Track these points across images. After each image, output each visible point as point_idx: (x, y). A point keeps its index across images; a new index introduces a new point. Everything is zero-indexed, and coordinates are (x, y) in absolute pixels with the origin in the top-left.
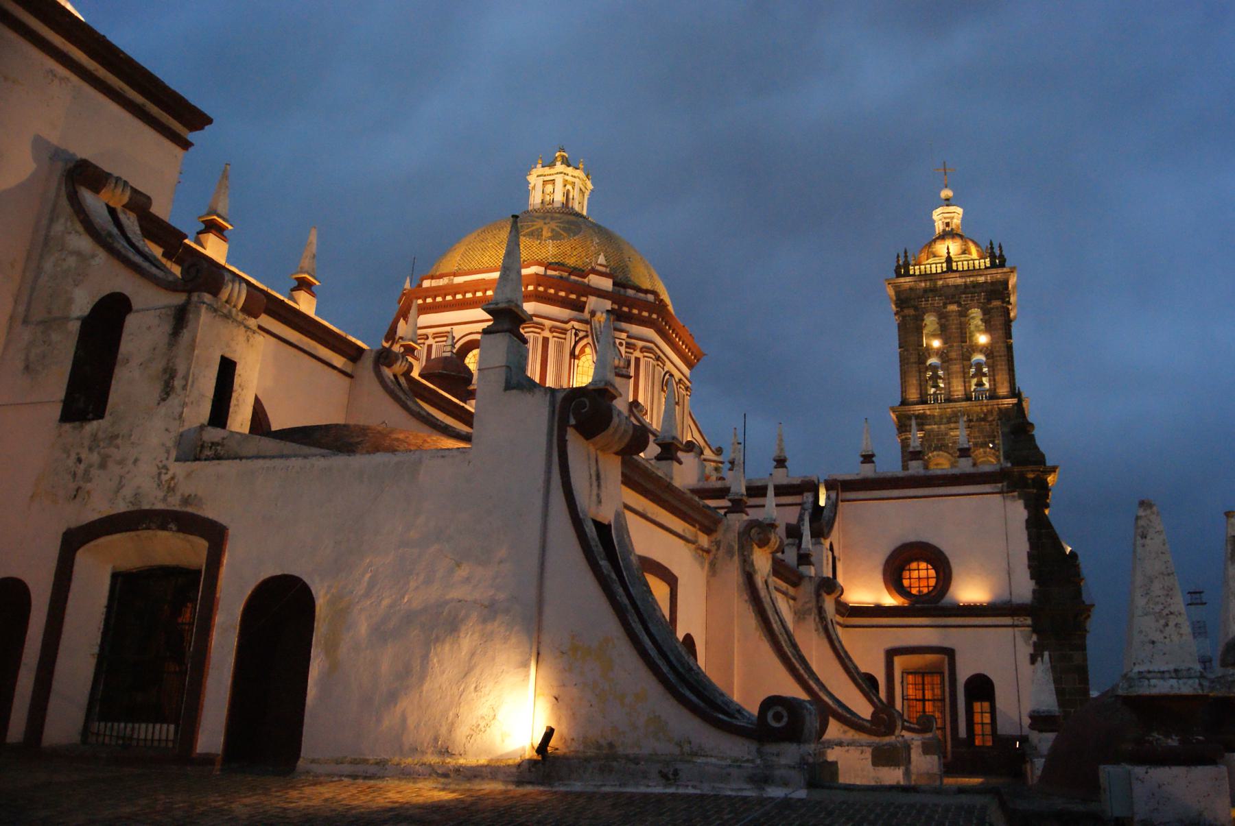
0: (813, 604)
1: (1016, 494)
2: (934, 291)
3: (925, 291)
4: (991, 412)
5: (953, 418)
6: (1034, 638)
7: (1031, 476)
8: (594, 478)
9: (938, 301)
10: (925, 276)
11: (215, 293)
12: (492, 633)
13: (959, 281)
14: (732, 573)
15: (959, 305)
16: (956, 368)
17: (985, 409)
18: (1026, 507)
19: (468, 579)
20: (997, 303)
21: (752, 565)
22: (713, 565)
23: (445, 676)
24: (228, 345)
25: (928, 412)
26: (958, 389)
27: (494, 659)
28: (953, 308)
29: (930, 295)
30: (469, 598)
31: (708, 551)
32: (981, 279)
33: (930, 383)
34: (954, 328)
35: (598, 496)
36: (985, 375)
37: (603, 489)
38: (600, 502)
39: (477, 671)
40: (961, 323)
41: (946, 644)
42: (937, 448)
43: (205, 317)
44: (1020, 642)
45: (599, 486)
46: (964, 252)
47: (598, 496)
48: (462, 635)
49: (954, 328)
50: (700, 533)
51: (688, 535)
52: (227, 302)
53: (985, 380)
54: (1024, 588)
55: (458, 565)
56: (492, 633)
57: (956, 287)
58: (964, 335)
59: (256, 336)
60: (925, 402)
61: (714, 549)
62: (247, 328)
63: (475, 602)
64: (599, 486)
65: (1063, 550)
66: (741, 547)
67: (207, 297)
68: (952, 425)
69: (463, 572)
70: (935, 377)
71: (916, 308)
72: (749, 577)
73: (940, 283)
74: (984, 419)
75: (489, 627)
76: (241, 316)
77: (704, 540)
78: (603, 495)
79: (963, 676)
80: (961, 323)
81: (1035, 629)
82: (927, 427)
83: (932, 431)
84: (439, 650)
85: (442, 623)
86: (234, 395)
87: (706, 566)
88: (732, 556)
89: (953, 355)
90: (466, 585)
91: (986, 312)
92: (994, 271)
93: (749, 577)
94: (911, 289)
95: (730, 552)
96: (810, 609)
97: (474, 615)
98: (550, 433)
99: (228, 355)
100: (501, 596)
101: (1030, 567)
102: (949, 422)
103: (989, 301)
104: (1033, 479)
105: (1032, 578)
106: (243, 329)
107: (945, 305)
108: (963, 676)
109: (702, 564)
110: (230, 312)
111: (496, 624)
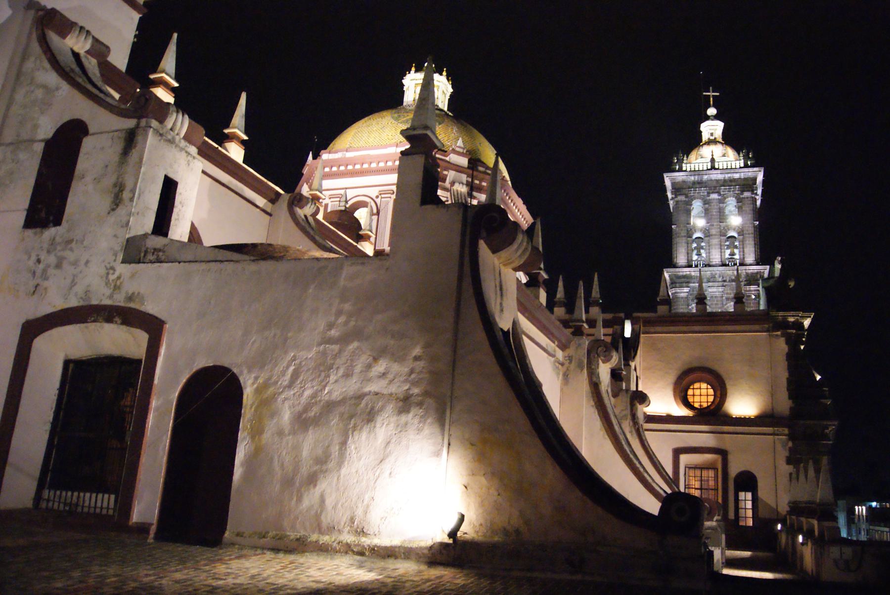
0: (628, 412)
1: (779, 333)
2: (700, 184)
3: (694, 183)
5: (712, 279)
6: (790, 444)
7: (791, 319)
8: (498, 288)
9: (703, 191)
10: (694, 172)
11: (162, 121)
12: (406, 424)
13: (720, 177)
14: (582, 382)
15: (720, 194)
16: (715, 241)
18: (787, 343)
19: (384, 374)
20: (747, 194)
21: (598, 377)
22: (566, 376)
23: (362, 462)
24: (171, 166)
26: (716, 258)
27: (407, 447)
28: (714, 196)
30: (385, 392)
31: (562, 364)
32: (737, 176)
33: (695, 252)
34: (714, 212)
35: (501, 304)
36: (736, 247)
37: (504, 298)
38: (502, 310)
39: (391, 459)
40: (720, 208)
41: (723, 447)
43: (151, 138)
44: (779, 447)
45: (502, 295)
46: (724, 156)
47: (501, 304)
48: (378, 425)
49: (714, 212)
50: (557, 349)
51: (549, 349)
52: (171, 129)
53: (736, 251)
54: (784, 404)
55: (375, 359)
56: (406, 424)
57: (717, 181)
58: (722, 217)
59: (195, 161)
60: (690, 266)
61: (567, 365)
62: (188, 154)
63: (391, 394)
64: (502, 295)
65: (815, 378)
66: (589, 363)
67: (154, 123)
68: (710, 284)
69: (380, 367)
70: (699, 248)
71: (687, 196)
72: (595, 386)
73: (705, 177)
75: (404, 418)
76: (183, 144)
77: (560, 354)
78: (504, 305)
79: (733, 471)
80: (720, 208)
81: (792, 437)
82: (691, 285)
84: (356, 438)
85: (360, 412)
86: (175, 210)
87: (561, 376)
88: (582, 370)
89: (714, 231)
90: (387, 377)
91: (739, 200)
92: (746, 170)
93: (595, 386)
94: (684, 182)
95: (580, 366)
96: (625, 416)
97: (390, 408)
98: (462, 246)
99: (171, 175)
100: (416, 391)
101: (788, 390)
103: (742, 192)
104: (793, 322)
105: (790, 398)
106: (185, 154)
107: (709, 194)
108: (733, 471)
109: (558, 374)
110: (174, 138)
111: (411, 415)
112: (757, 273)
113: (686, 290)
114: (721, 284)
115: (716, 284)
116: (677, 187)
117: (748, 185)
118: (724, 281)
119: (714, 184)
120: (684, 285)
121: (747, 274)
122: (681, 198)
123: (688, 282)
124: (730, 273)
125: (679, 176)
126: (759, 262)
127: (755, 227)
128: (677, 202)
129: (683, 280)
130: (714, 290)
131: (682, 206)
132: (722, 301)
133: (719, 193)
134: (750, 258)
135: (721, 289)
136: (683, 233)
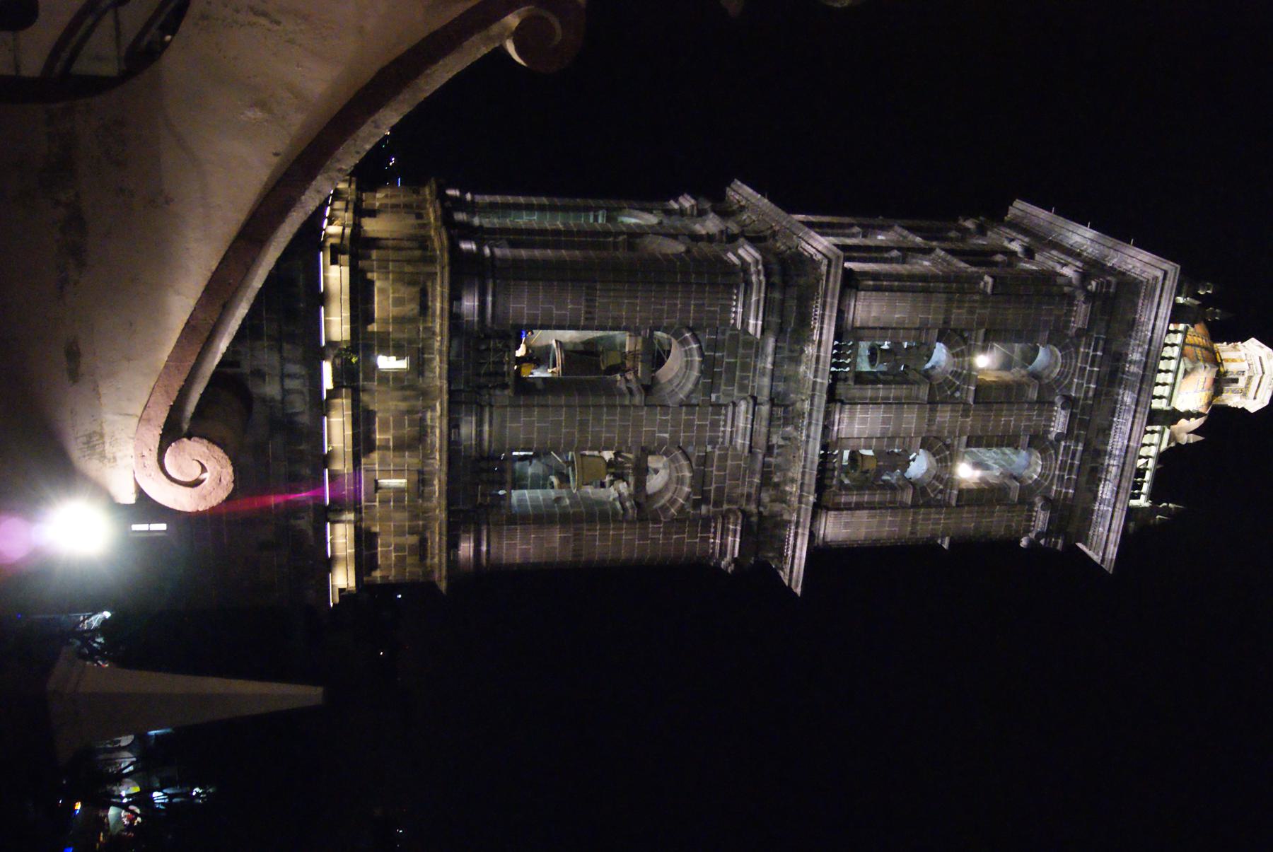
2: (1112, 376)
4: (782, 498)
5: (782, 408)
9: (1083, 387)
17: (793, 489)
25: (810, 350)
29: (1105, 369)
34: (1009, 419)
42: (709, 367)
57: (1105, 431)
60: (838, 336)
68: (765, 409)
71: (1080, 333)
73: (1128, 398)
74: (766, 480)
82: (771, 343)
83: (756, 348)
89: (945, 416)
91: (1027, 493)
102: (776, 400)
103: (1049, 503)
107: (1069, 402)
112: (781, 556)
113: (755, 325)
114: (762, 440)
115: (762, 428)
117: (1072, 516)
118: (769, 449)
119: (1099, 421)
120: (775, 320)
122: (1080, 315)
123: (780, 333)
124: (796, 471)
125: (1155, 317)
126: (820, 554)
128: (1070, 299)
132: (700, 443)
133: (1068, 435)
134: (833, 528)
136: (959, 315)
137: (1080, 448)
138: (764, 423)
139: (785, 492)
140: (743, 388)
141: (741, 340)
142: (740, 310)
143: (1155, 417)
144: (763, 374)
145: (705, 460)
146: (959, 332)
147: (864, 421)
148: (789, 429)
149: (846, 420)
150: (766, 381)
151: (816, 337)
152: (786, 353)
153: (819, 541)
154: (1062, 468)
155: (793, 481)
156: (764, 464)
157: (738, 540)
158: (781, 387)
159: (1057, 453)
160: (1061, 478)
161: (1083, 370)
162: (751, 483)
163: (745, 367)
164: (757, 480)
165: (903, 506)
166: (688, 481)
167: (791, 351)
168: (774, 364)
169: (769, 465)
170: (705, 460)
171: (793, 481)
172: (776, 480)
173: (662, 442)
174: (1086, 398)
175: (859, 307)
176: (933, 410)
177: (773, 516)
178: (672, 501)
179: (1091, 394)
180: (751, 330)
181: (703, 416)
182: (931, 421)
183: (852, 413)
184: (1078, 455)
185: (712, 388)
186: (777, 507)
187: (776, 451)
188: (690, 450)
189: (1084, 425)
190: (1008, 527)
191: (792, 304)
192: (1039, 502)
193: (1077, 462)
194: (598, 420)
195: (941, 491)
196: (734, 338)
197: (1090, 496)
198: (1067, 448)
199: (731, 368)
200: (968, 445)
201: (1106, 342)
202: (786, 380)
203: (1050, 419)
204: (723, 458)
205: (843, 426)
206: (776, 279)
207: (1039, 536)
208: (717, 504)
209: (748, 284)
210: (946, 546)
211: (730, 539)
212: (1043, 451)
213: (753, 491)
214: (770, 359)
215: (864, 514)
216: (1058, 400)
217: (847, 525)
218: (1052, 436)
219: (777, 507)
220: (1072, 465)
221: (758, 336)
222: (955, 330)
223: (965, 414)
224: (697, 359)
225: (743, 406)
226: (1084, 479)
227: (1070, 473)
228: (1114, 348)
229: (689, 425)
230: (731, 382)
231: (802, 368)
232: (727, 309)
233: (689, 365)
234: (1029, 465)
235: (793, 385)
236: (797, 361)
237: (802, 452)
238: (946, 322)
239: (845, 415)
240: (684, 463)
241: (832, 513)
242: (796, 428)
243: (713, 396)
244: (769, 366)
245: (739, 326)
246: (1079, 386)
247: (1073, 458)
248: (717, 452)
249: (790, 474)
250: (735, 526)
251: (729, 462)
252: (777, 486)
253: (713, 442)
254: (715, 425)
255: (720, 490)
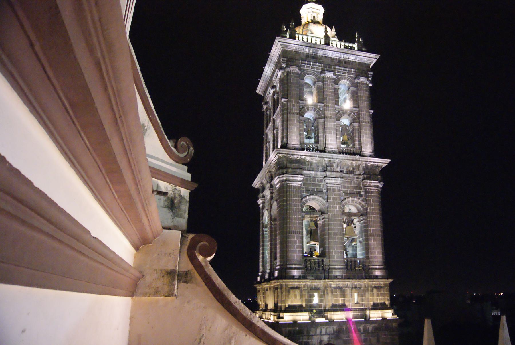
2: (314, 58)
3: (308, 56)
4: (358, 167)
9: (318, 67)
17: (355, 164)
25: (308, 159)
28: (329, 75)
29: (311, 60)
34: (329, 91)
42: (315, 192)
57: (332, 59)
60: (303, 149)
68: (328, 173)
73: (321, 52)
82: (306, 172)
83: (308, 176)
89: (328, 113)
94: (296, 52)
103: (357, 77)
107: (323, 72)
112: (378, 167)
113: (300, 178)
114: (339, 174)
116: (289, 56)
117: (361, 69)
118: (341, 171)
119: (329, 61)
120: (298, 171)
121: (367, 166)
122: (294, 69)
125: (293, 45)
126: (377, 153)
127: (370, 116)
128: (288, 73)
129: (297, 165)
130: (332, 181)
131: (294, 80)
134: (368, 149)
135: (339, 181)
136: (295, 110)
137: (338, 67)
138: (333, 173)
139: (356, 166)
140: (321, 181)
141: (305, 182)
142: (295, 183)
143: (327, 43)
144: (316, 174)
145: (346, 193)
146: (300, 110)
147: (331, 140)
148: (334, 165)
149: (331, 146)
150: (319, 173)
151: (303, 157)
152: (309, 167)
153: (372, 154)
154: (345, 73)
155: (352, 163)
156: (347, 173)
157: (372, 181)
158: (320, 168)
159: (340, 75)
160: (348, 74)
161: (312, 68)
162: (354, 178)
163: (314, 180)
164: (352, 175)
165: (359, 126)
166: (353, 199)
167: (308, 165)
168: (313, 171)
169: (347, 171)
170: (346, 193)
171: (352, 163)
172: (352, 169)
173: (340, 208)
174: (321, 66)
175: (293, 143)
176: (327, 117)
177: (364, 169)
178: (360, 204)
179: (320, 65)
180: (302, 179)
181: (331, 194)
182: (330, 118)
183: (328, 144)
184: (341, 68)
185: (322, 192)
186: (361, 169)
187: (342, 169)
188: (342, 198)
189: (330, 66)
190: (366, 91)
191: (293, 165)
192: (356, 81)
193: (343, 68)
194: (333, 229)
195: (354, 114)
196: (304, 184)
197: (354, 64)
198: (338, 72)
199: (315, 185)
200: (338, 105)
201: (302, 60)
202: (318, 167)
203: (329, 78)
204: (345, 187)
205: (333, 147)
206: (285, 171)
207: (368, 80)
208: (360, 188)
209: (286, 180)
210: (372, 111)
211: (372, 184)
212: (339, 80)
213: (356, 177)
214: (311, 172)
215: (362, 139)
216: (322, 75)
217: (366, 145)
218: (335, 77)
219: (361, 169)
220: (344, 70)
221: (303, 176)
222: (300, 111)
223: (328, 106)
224: (312, 197)
225: (327, 181)
226: (349, 66)
227: (347, 71)
228: (304, 58)
229: (334, 199)
230: (319, 185)
231: (314, 161)
232: (295, 187)
233: (314, 199)
234: (344, 85)
235: (320, 164)
236: (311, 164)
237: (342, 161)
238: (297, 114)
239: (329, 146)
240: (347, 200)
241: (362, 150)
242: (334, 163)
243: (324, 191)
244: (314, 172)
245: (300, 183)
246: (317, 69)
247: (341, 70)
248: (343, 189)
249: (350, 164)
250: (368, 183)
251: (346, 185)
252: (354, 169)
253: (339, 190)
254: (334, 190)
255: (356, 188)
